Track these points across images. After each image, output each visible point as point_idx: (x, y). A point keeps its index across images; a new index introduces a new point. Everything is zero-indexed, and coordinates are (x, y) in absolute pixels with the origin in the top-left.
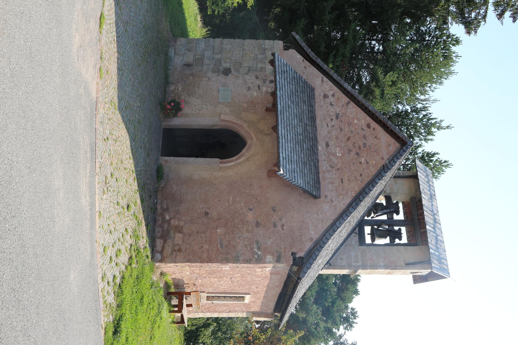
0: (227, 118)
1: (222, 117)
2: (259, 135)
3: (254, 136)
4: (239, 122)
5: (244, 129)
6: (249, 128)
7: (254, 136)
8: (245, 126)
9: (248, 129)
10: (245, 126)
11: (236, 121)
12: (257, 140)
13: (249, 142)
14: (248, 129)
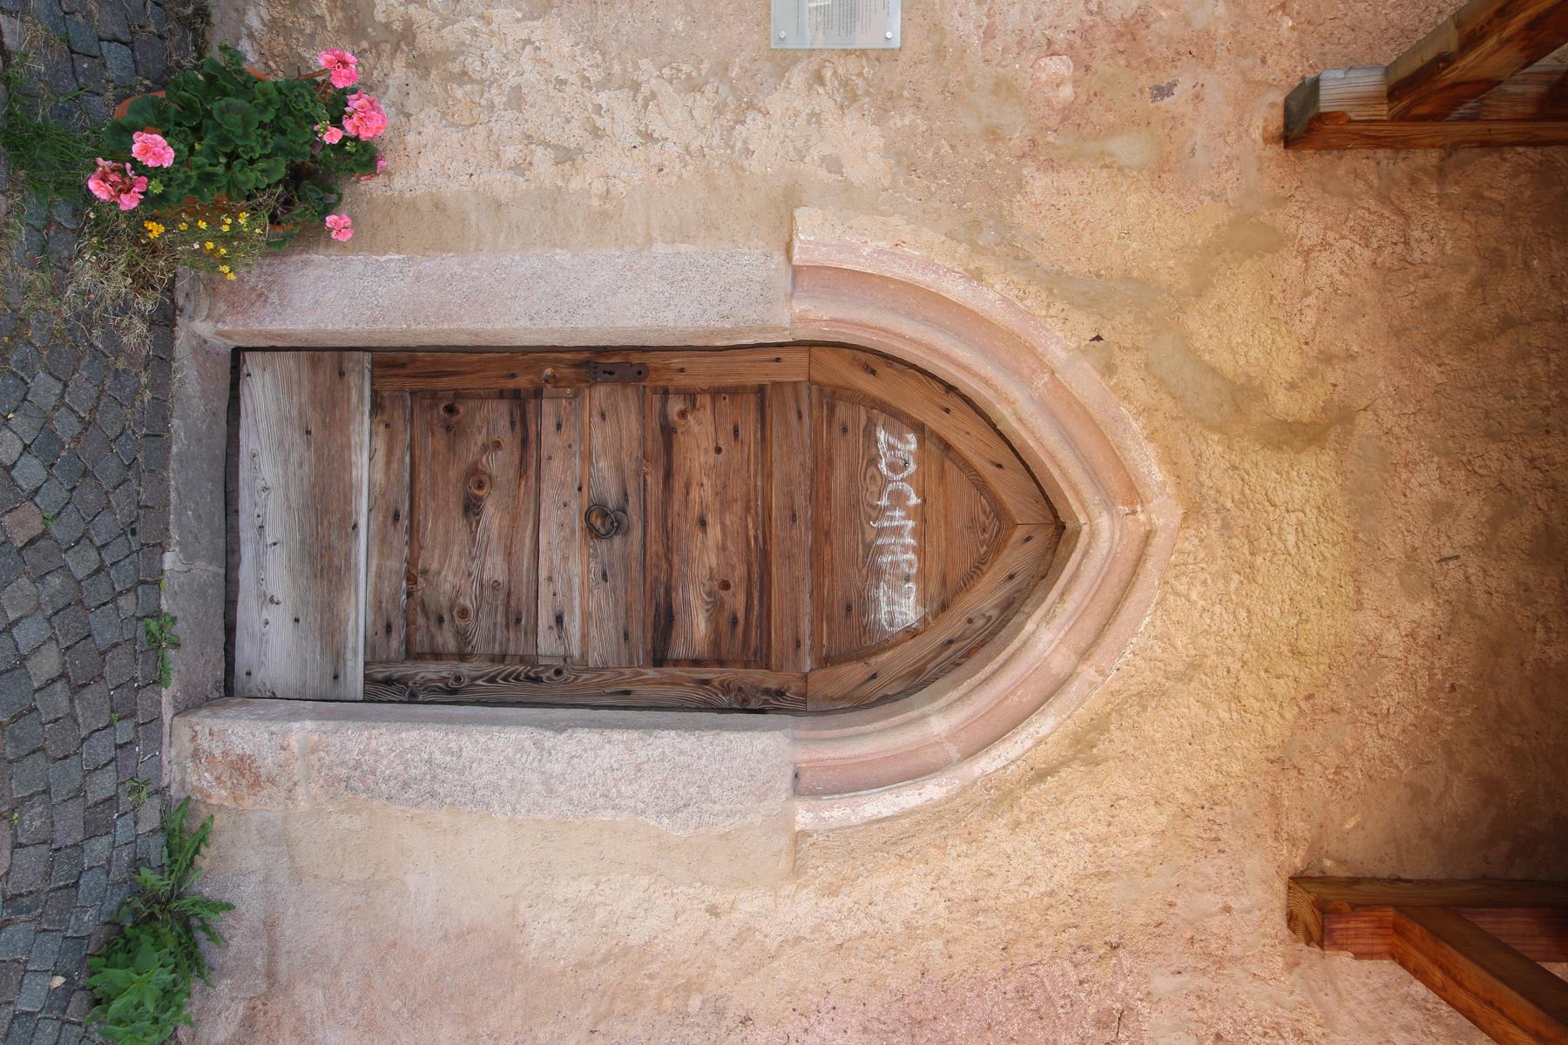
0: (864, 244)
1: (817, 236)
2: (1213, 447)
3: (1152, 470)
4: (989, 299)
5: (1045, 373)
6: (1109, 369)
7: (1152, 470)
8: (1060, 342)
9: (1085, 382)
10: (1060, 342)
11: (956, 289)
12: (1193, 512)
13: (1102, 532)
14: (1085, 382)
